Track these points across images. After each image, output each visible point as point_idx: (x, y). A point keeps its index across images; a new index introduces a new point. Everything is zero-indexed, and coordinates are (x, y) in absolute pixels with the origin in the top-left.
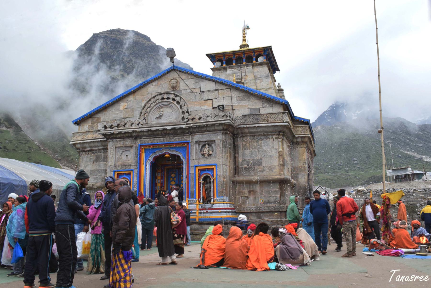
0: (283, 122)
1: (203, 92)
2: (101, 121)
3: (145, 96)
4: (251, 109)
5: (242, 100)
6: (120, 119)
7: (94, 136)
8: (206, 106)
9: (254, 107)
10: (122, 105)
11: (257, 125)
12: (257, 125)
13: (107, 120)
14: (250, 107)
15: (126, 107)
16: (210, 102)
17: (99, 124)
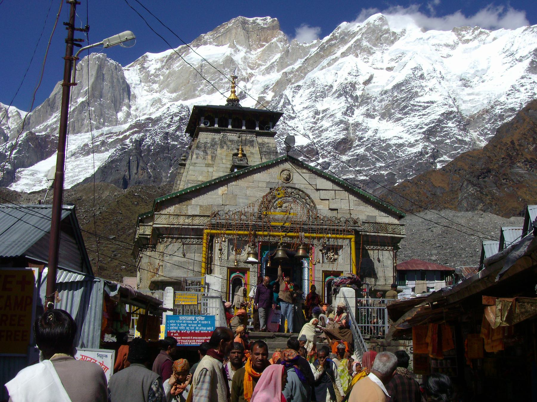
0: (400, 234)
1: (319, 190)
2: (193, 203)
3: (251, 184)
4: (368, 216)
5: (359, 205)
6: (218, 206)
7: (187, 221)
8: (322, 206)
9: (371, 215)
10: (221, 190)
11: (376, 234)
12: (376, 234)
13: (201, 203)
14: (367, 214)
15: (226, 192)
16: (327, 202)
17: (189, 207)
